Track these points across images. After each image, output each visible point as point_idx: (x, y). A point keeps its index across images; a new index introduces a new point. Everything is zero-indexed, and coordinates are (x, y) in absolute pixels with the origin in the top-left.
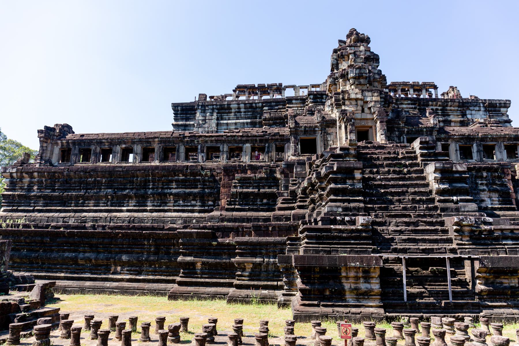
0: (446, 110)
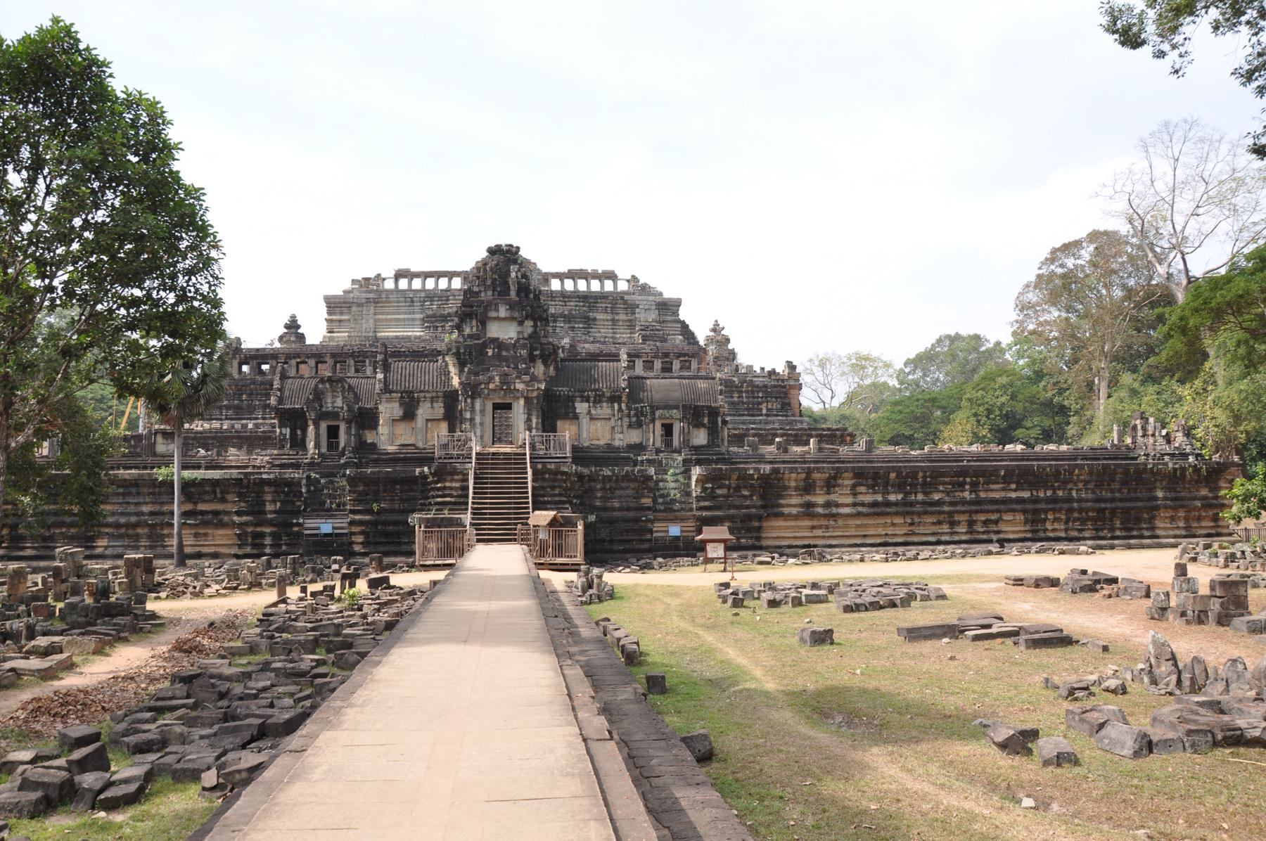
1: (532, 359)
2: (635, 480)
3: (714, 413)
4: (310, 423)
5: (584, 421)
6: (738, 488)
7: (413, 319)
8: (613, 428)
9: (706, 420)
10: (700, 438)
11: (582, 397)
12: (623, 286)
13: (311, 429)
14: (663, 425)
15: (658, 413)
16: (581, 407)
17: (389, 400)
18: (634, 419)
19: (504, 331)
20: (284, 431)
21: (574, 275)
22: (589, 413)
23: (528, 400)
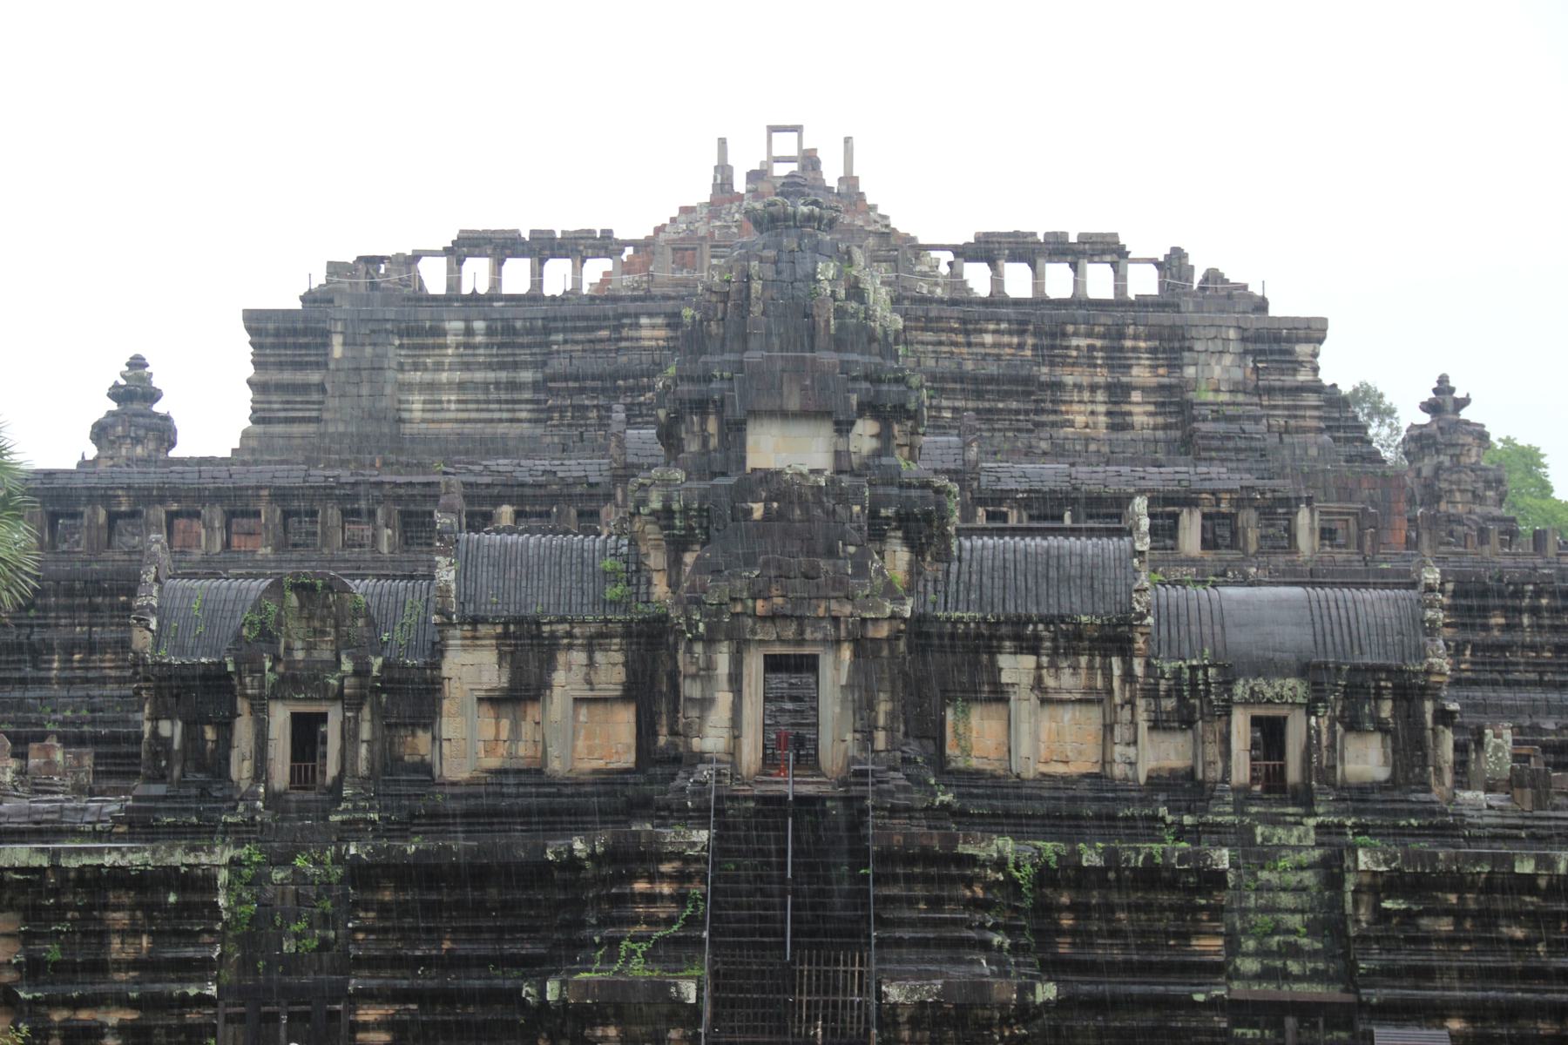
0: (1121, 349)
1: (877, 532)
2: (1172, 885)
3: (1409, 691)
4: (243, 706)
5: (1024, 705)
6: (1487, 918)
7: (513, 386)
8: (1108, 728)
9: (1386, 709)
10: (1366, 760)
11: (1017, 637)
12: (1143, 282)
13: (244, 729)
14: (1256, 722)
15: (1240, 690)
16: (1015, 668)
17: (474, 641)
18: (1169, 704)
20: (165, 728)
21: (987, 249)
23: (862, 646)
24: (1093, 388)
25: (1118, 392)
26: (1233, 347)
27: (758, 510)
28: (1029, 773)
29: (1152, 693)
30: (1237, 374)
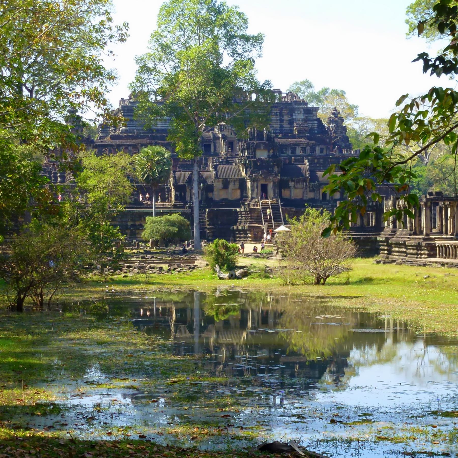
8: (303, 192)
16: (291, 184)
19: (262, 154)
22: (294, 186)
23: (274, 183)
24: (277, 120)
25: (281, 121)
26: (302, 112)
27: (259, 164)
28: (293, 198)
29: (310, 187)
30: (303, 117)
